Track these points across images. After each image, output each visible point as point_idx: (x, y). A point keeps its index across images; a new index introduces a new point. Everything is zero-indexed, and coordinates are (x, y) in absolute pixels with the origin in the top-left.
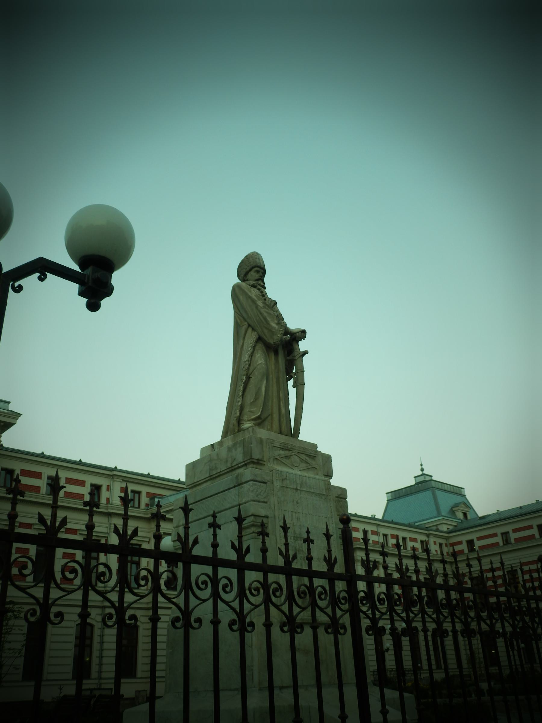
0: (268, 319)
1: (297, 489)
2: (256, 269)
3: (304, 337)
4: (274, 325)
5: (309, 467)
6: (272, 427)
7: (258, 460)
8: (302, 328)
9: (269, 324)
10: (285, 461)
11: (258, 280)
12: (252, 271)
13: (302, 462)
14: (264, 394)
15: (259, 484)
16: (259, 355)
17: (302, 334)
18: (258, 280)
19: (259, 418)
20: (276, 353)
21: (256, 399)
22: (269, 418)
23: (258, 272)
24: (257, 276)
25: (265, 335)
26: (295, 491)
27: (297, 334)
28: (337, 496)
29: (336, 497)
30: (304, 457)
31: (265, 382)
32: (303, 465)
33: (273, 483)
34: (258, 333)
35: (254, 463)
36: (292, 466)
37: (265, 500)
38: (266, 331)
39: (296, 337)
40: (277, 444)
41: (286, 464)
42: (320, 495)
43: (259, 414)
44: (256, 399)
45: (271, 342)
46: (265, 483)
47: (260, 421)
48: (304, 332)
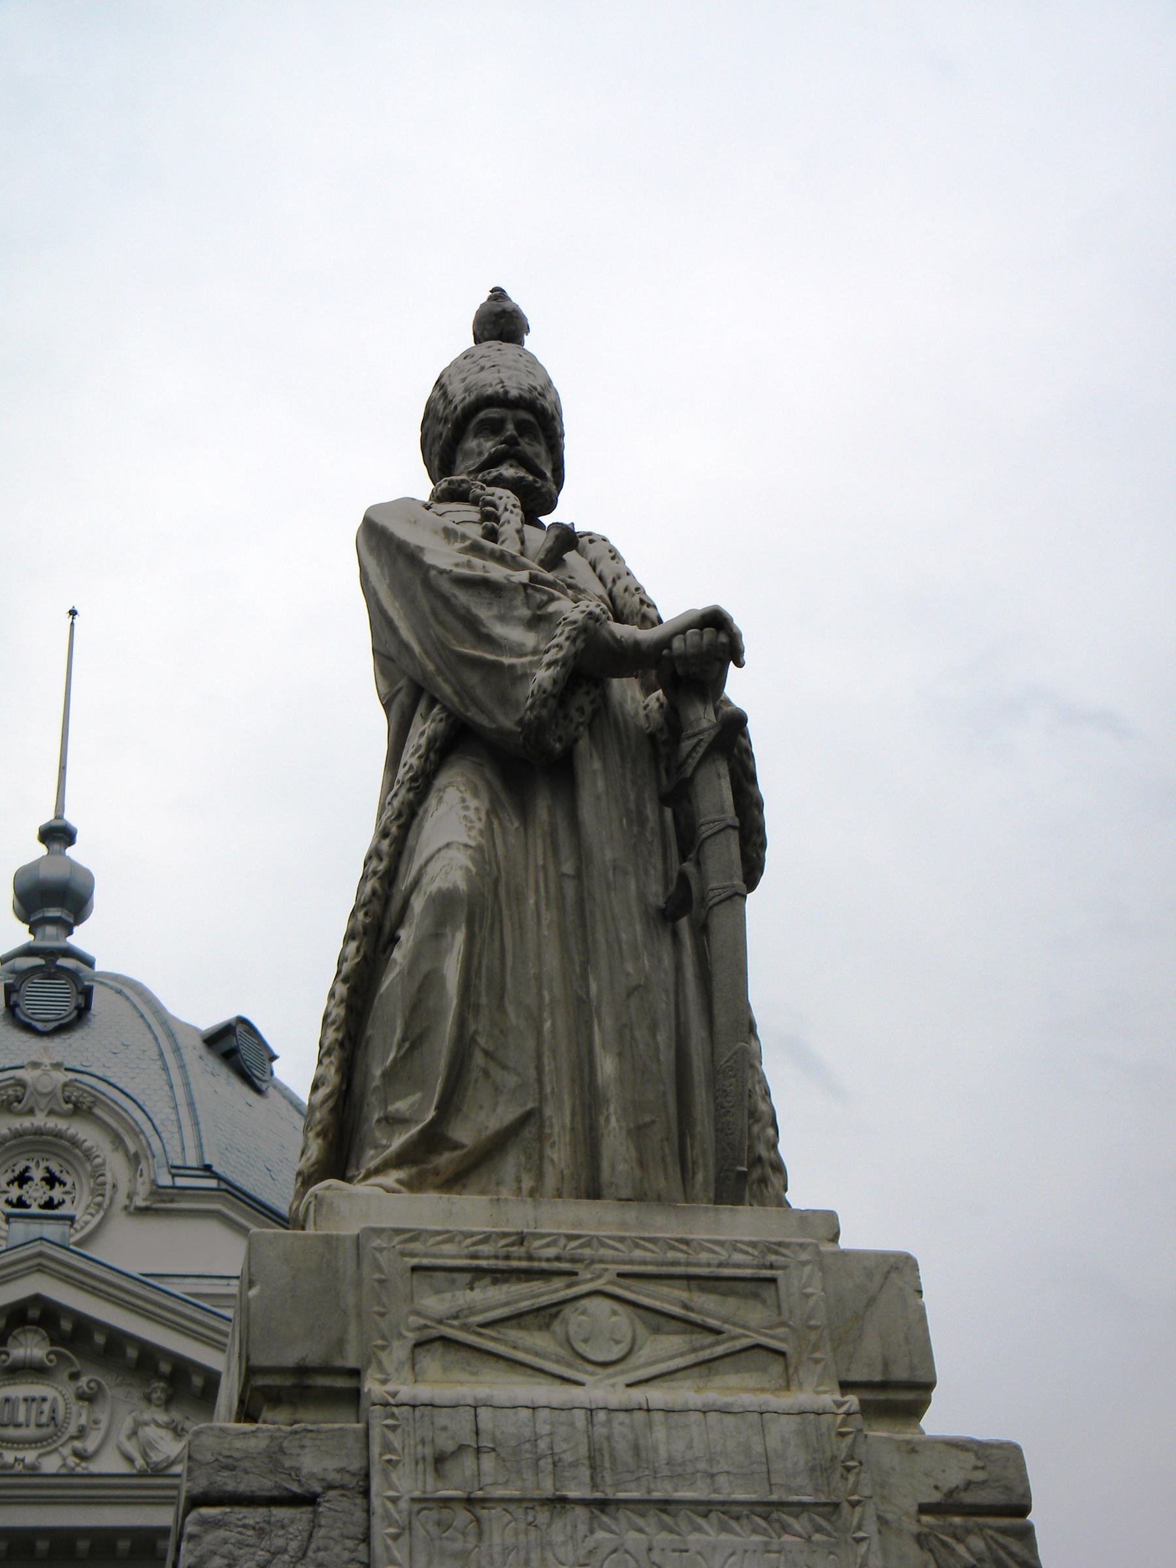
2: (481, 415)
3: (733, 651)
5: (720, 1350)
6: (540, 1176)
7: (302, 1370)
8: (701, 603)
10: (535, 1342)
11: (495, 461)
12: (494, 432)
13: (656, 1330)
14: (454, 1003)
15: (253, 1516)
16: (443, 808)
17: (714, 641)
18: (495, 461)
19: (432, 1139)
20: (562, 772)
21: (414, 1042)
22: (529, 1132)
23: (493, 428)
24: (489, 446)
25: (476, 702)
26: (543, 1516)
27: (677, 644)
28: (935, 1497)
29: (924, 1509)
30: (667, 1297)
31: (460, 938)
32: (668, 1348)
33: (366, 1493)
34: (444, 708)
35: (275, 1398)
38: (473, 679)
39: (671, 659)
42: (769, 1511)
43: (431, 1114)
44: (414, 1042)
45: (507, 722)
46: (309, 1500)
47: (444, 1160)
48: (715, 621)
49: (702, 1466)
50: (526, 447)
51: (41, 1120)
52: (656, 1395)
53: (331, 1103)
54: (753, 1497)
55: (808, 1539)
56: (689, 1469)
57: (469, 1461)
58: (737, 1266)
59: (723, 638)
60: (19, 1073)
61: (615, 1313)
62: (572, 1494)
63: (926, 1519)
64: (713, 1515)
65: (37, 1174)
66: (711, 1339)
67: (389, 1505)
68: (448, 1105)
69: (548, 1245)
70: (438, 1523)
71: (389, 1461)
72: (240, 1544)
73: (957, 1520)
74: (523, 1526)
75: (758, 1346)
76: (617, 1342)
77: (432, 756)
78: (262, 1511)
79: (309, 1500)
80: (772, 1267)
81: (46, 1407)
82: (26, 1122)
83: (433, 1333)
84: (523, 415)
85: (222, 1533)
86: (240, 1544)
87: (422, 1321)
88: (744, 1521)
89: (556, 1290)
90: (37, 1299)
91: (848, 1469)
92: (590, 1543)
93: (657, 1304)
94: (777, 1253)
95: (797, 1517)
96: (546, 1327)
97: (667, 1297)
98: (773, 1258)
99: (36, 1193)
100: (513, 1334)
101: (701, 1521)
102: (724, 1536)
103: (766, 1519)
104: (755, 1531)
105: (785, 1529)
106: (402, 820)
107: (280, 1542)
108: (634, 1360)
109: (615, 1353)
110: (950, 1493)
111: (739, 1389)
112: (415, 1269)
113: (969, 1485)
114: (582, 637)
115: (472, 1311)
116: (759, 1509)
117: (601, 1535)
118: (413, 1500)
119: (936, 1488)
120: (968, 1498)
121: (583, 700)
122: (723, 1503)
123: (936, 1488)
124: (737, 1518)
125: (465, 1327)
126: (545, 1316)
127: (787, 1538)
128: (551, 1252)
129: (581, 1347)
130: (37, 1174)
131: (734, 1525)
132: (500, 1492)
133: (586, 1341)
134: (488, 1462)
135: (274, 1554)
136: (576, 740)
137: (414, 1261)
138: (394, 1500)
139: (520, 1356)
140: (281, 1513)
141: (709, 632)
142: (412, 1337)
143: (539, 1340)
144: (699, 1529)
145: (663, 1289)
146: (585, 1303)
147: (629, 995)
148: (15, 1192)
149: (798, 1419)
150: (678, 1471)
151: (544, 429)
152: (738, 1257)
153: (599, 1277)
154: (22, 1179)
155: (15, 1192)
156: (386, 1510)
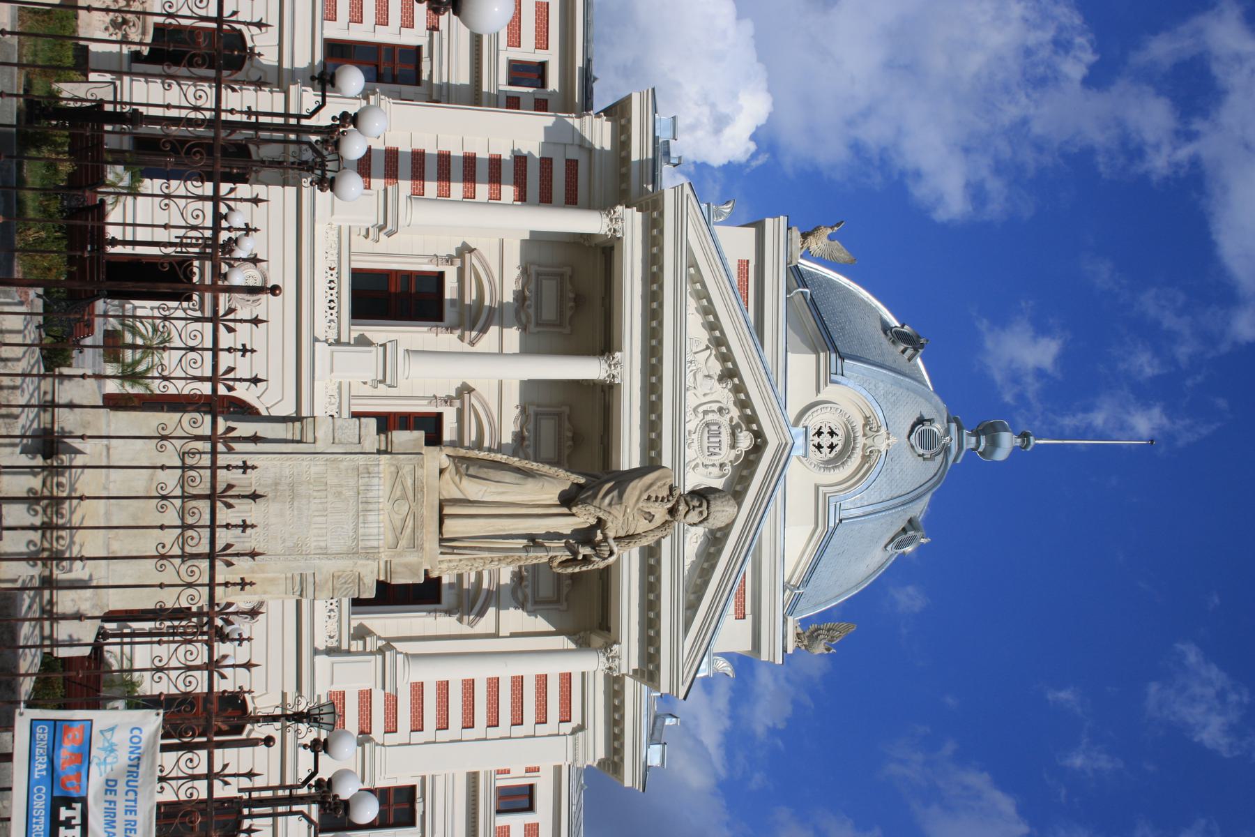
30: (410, 523)
32: (398, 524)
40: (419, 472)
51: (861, 441)
60: (883, 430)
65: (835, 440)
81: (717, 450)
82: (860, 433)
89: (411, 496)
90: (765, 442)
97: (410, 523)
99: (825, 440)
100: (400, 487)
130: (835, 440)
148: (825, 430)
154: (832, 433)
155: (825, 430)
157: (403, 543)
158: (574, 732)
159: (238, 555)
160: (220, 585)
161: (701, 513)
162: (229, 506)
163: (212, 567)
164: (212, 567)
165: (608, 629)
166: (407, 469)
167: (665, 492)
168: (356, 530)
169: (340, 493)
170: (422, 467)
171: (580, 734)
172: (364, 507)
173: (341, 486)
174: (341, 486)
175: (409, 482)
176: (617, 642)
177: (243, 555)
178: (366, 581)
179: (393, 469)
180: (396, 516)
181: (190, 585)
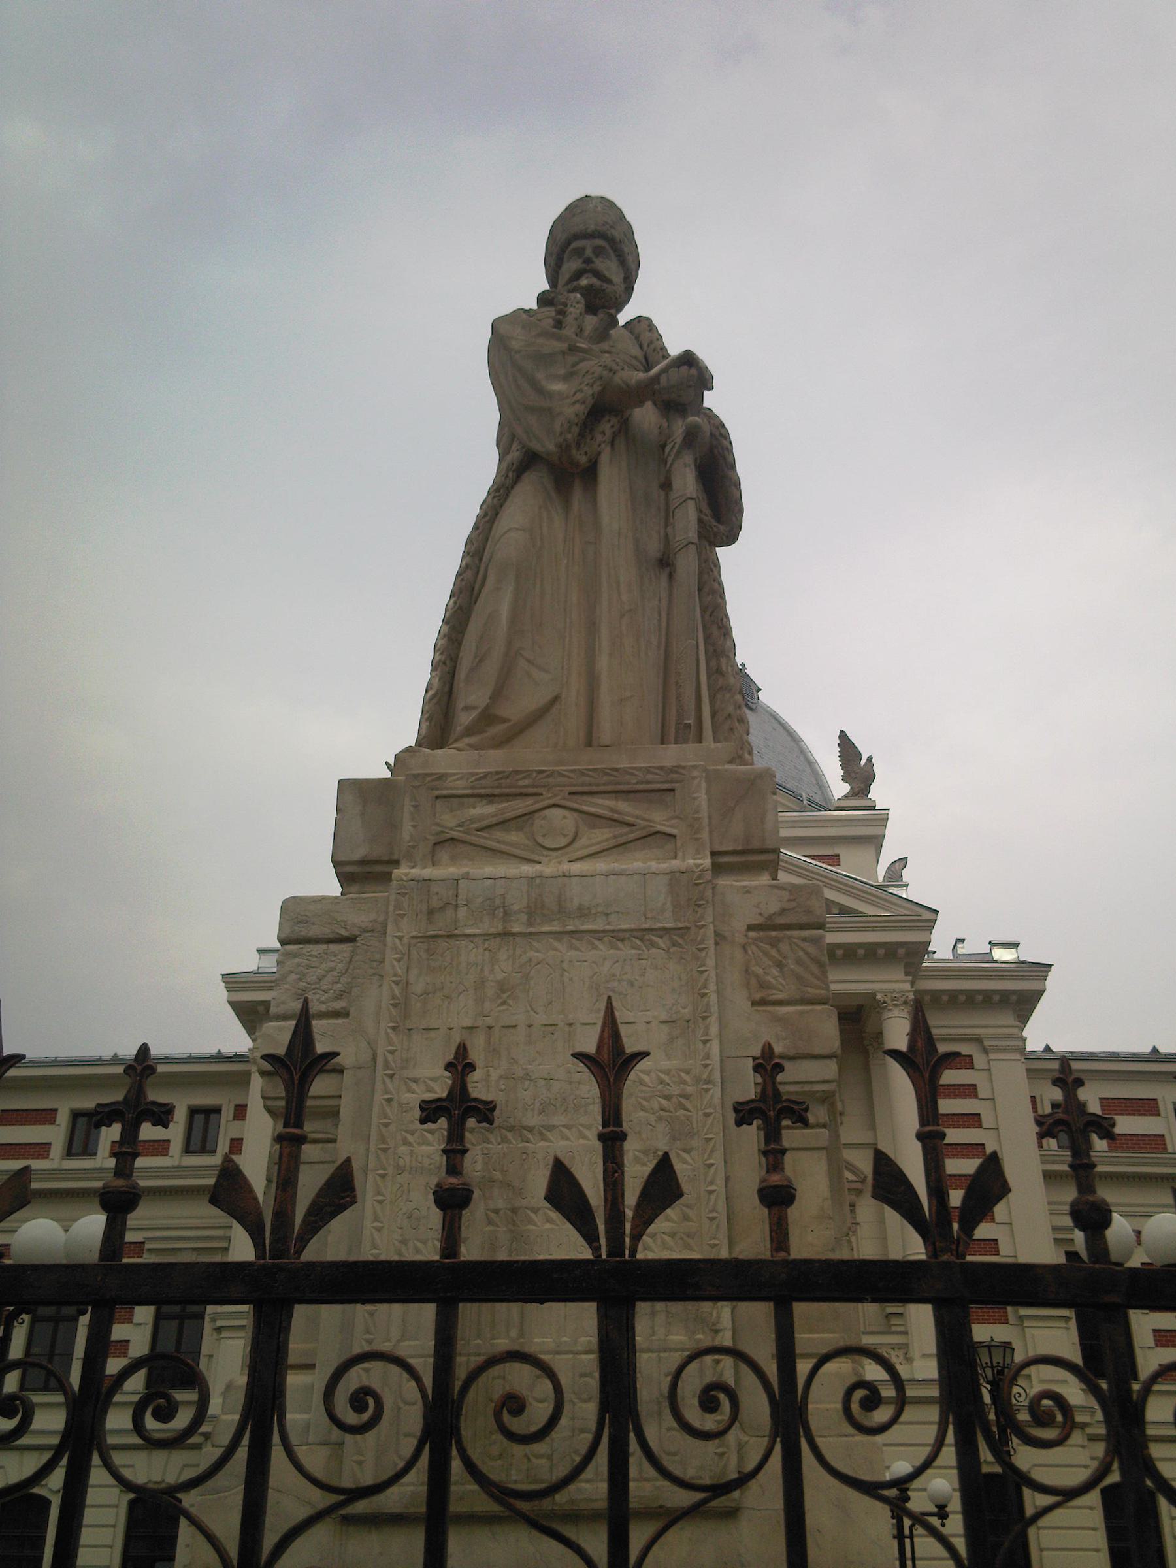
0: (540, 376)
1: (505, 934)
4: (558, 387)
5: (631, 836)
7: (363, 862)
9: (540, 391)
11: (578, 275)
18: (578, 275)
19: (488, 718)
20: (590, 473)
23: (579, 252)
28: (759, 920)
29: (750, 928)
30: (601, 805)
36: (538, 850)
37: (338, 1005)
40: (459, 786)
41: (494, 851)
42: (642, 935)
46: (351, 940)
47: (497, 729)
48: (688, 359)
49: (600, 909)
50: (600, 264)
52: (576, 867)
53: (435, 701)
54: (633, 926)
55: (668, 951)
56: (593, 911)
57: (450, 912)
58: (648, 782)
59: (694, 371)
61: (565, 817)
62: (515, 930)
63: (752, 934)
64: (606, 939)
66: (626, 829)
67: (397, 941)
68: (497, 695)
69: (524, 778)
70: (427, 950)
71: (399, 915)
72: (308, 967)
73: (774, 933)
74: (481, 950)
75: (658, 832)
76: (565, 836)
77: (510, 474)
78: (324, 946)
79: (351, 940)
80: (672, 782)
83: (448, 836)
84: (599, 242)
85: (297, 960)
86: (308, 967)
87: (440, 829)
88: (626, 942)
89: (527, 804)
91: (699, 906)
92: (524, 959)
93: (592, 810)
94: (677, 772)
95: (661, 937)
96: (520, 829)
98: (675, 776)
100: (498, 834)
101: (597, 942)
102: (612, 951)
103: (642, 940)
104: (633, 948)
105: (653, 945)
106: (487, 519)
107: (332, 965)
108: (576, 845)
109: (563, 842)
110: (770, 917)
111: (636, 862)
112: (437, 797)
113: (783, 911)
114: (598, 383)
115: (472, 821)
116: (635, 934)
117: (532, 954)
118: (413, 937)
119: (761, 914)
120: (781, 920)
121: (607, 427)
122: (613, 931)
123: (761, 914)
124: (622, 940)
125: (467, 832)
126: (522, 820)
127: (654, 950)
128: (526, 782)
129: (540, 840)
131: (620, 944)
132: (468, 931)
133: (544, 836)
134: (462, 913)
135: (328, 972)
136: (599, 454)
137: (437, 793)
138: (400, 938)
139: (503, 847)
140: (334, 947)
141: (684, 369)
142: (432, 839)
143: (514, 837)
144: (595, 948)
145: (599, 800)
146: (547, 812)
147: (622, 616)
149: (668, 877)
150: (583, 913)
151: (615, 250)
152: (650, 777)
153: (556, 796)
156: (395, 944)
157: (659, 819)
158: (986, 1051)
159: (612, 1140)
160: (780, 1234)
161: (598, 251)
162: (340, 1191)
163: (683, 1281)
164: (683, 1281)
165: (860, 1008)
166: (449, 819)
167: (550, 311)
168: (617, 936)
169: (502, 987)
170: (442, 777)
171: (986, 1043)
172: (548, 917)
173: (481, 984)
174: (481, 984)
175: (485, 811)
176: (874, 996)
177: (612, 1114)
178: (774, 907)
179: (444, 855)
180: (583, 841)
181: (790, 1418)
